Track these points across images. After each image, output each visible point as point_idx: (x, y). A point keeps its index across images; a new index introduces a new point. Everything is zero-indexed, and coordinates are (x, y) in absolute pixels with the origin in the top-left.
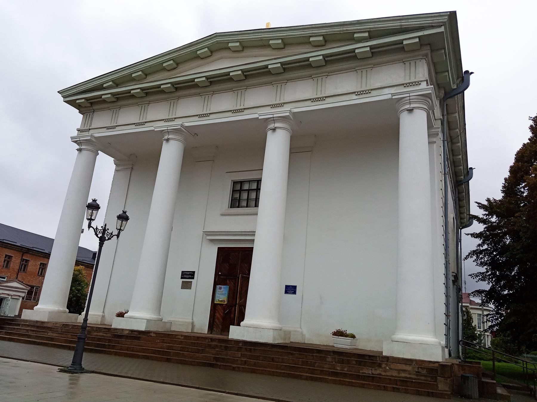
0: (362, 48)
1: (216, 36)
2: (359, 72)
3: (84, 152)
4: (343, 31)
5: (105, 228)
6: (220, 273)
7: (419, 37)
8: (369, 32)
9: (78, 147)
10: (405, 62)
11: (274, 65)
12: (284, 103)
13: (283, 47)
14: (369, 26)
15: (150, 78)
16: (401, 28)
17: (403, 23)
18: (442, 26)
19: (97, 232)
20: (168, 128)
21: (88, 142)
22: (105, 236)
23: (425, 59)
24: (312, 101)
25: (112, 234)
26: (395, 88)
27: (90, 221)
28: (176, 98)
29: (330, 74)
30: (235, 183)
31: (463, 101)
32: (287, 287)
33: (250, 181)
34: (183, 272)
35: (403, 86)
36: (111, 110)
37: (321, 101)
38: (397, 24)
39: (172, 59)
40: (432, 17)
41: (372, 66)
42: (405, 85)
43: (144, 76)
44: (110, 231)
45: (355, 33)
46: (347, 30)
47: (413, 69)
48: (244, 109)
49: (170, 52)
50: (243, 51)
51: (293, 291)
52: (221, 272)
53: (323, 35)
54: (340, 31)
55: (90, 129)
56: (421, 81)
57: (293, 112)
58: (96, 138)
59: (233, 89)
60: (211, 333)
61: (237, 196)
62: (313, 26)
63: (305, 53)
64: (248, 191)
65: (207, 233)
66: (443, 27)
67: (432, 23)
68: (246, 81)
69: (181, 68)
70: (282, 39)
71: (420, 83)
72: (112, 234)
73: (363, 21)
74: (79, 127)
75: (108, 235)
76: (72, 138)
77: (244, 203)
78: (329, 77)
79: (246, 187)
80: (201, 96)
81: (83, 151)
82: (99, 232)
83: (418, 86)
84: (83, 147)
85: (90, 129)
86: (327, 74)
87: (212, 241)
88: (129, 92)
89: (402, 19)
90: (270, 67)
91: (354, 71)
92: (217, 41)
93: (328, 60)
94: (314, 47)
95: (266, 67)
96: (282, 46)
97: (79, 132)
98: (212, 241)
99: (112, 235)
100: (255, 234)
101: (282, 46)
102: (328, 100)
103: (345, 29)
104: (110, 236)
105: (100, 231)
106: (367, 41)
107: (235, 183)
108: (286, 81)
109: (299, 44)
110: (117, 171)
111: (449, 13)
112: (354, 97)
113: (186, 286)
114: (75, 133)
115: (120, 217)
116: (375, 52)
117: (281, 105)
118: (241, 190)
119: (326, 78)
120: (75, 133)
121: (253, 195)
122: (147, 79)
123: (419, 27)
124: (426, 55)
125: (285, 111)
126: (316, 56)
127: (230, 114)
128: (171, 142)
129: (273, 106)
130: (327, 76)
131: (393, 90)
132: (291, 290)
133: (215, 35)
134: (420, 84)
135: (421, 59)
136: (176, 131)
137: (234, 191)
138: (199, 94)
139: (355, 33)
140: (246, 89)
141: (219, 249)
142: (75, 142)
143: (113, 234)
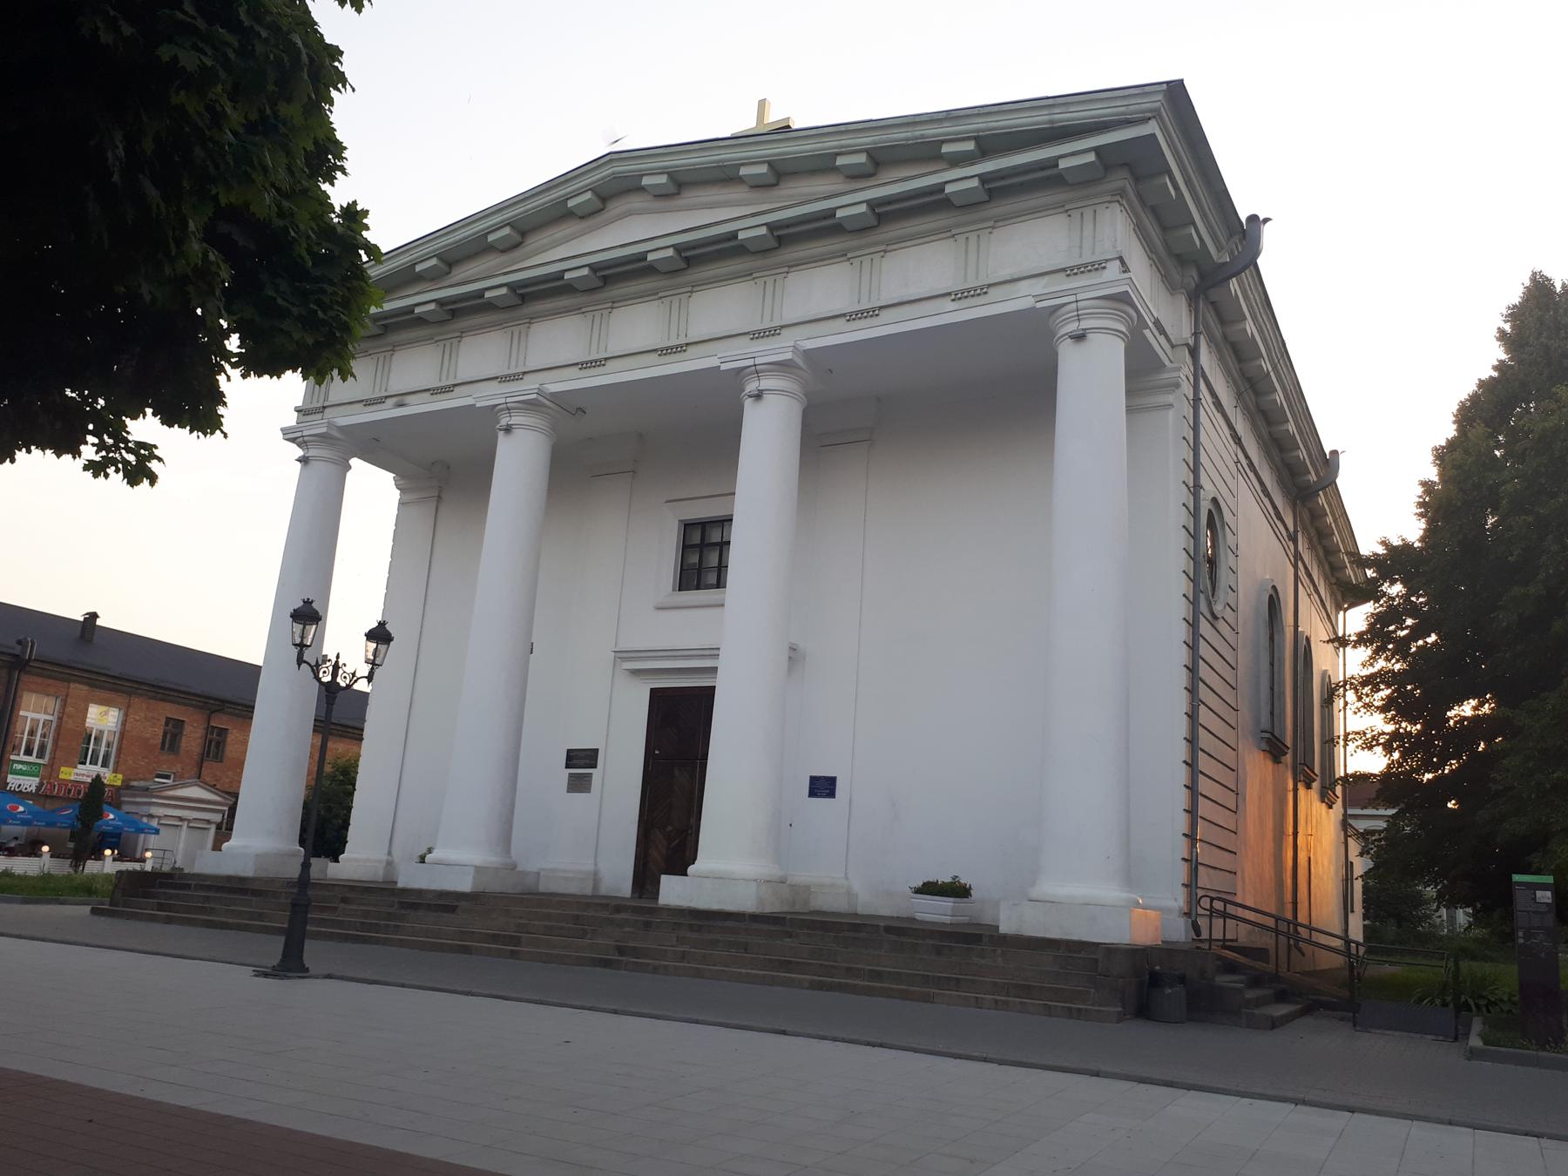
2: (961, 238)
3: (314, 465)
5: (337, 662)
6: (657, 752)
7: (1097, 150)
8: (975, 138)
9: (299, 452)
10: (1069, 213)
12: (782, 327)
13: (775, 182)
15: (461, 273)
18: (1149, 119)
19: (319, 673)
20: (509, 400)
21: (323, 438)
22: (339, 680)
23: (1118, 201)
25: (354, 674)
26: (1046, 279)
27: (301, 650)
29: (889, 248)
30: (688, 526)
31: (1260, 289)
32: (813, 780)
34: (569, 751)
35: (1063, 274)
38: (1040, 119)
39: (508, 224)
40: (1124, 97)
41: (991, 223)
42: (1069, 272)
43: (446, 269)
44: (349, 669)
45: (943, 142)
46: (922, 136)
47: (1088, 227)
48: (687, 344)
49: (502, 206)
50: (679, 194)
51: (828, 791)
52: (658, 750)
54: (907, 139)
55: (324, 407)
56: (1107, 261)
57: (804, 351)
58: (341, 429)
59: (660, 295)
60: (640, 897)
61: (694, 559)
62: (842, 128)
65: (622, 655)
66: (1153, 123)
67: (1123, 114)
68: (690, 271)
69: (534, 242)
70: (770, 163)
71: (1104, 265)
72: (354, 674)
74: (299, 403)
75: (345, 677)
78: (888, 254)
80: (583, 313)
81: (313, 462)
82: (325, 672)
83: (1099, 272)
84: (312, 453)
85: (324, 407)
86: (883, 247)
88: (409, 310)
90: (741, 236)
91: (948, 237)
92: (613, 173)
93: (885, 214)
95: (733, 235)
96: (772, 180)
99: (355, 678)
100: (718, 655)
101: (772, 180)
102: (886, 315)
103: (918, 133)
104: (350, 681)
105: (325, 669)
106: (973, 164)
107: (688, 526)
108: (786, 269)
110: (401, 503)
111: (1165, 86)
112: (947, 304)
113: (579, 784)
115: (370, 636)
117: (773, 332)
119: (882, 257)
120: (291, 420)
122: (450, 275)
124: (1122, 193)
126: (852, 203)
127: (654, 357)
128: (517, 433)
129: (757, 335)
130: (885, 251)
131: (1039, 286)
132: (823, 787)
134: (1104, 268)
135: (1110, 202)
136: (530, 406)
137: (686, 547)
138: (577, 310)
139: (943, 142)
140: (692, 292)
141: (654, 692)
142: (293, 440)
143: (358, 675)
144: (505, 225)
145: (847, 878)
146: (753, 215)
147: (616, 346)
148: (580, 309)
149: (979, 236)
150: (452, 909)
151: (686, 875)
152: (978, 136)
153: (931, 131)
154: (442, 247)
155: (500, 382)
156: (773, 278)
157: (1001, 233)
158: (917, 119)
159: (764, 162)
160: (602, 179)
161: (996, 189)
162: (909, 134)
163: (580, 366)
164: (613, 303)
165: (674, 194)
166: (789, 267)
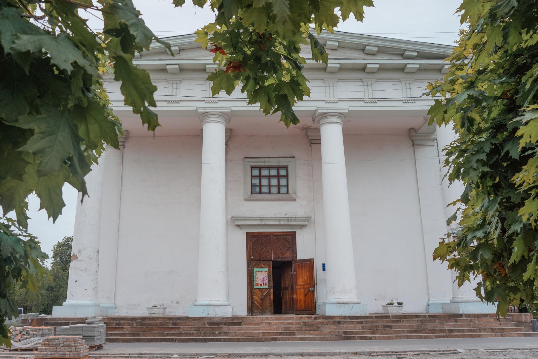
0: (413, 64)
4: (396, 47)
6: (252, 258)
14: (419, 48)
15: (184, 55)
24: (326, 103)
28: (179, 80)
29: (378, 80)
33: (269, 168)
37: (409, 103)
46: (400, 47)
54: (394, 46)
64: (269, 177)
65: (234, 219)
73: (412, 42)
79: (265, 172)
87: (238, 226)
89: (445, 48)
93: (383, 69)
94: (365, 54)
98: (238, 226)
109: (350, 49)
112: (401, 103)
118: (260, 177)
121: (283, 182)
125: (343, 107)
145: (115, 304)
146: (335, 59)
147: (378, 95)
149: (329, 83)
151: (62, 306)
153: (404, 46)
155: (206, 103)
156: (332, 82)
157: (340, 83)
158: (399, 41)
159: (337, 41)
162: (395, 45)
163: (168, 102)
164: (415, 79)
166: (415, 79)
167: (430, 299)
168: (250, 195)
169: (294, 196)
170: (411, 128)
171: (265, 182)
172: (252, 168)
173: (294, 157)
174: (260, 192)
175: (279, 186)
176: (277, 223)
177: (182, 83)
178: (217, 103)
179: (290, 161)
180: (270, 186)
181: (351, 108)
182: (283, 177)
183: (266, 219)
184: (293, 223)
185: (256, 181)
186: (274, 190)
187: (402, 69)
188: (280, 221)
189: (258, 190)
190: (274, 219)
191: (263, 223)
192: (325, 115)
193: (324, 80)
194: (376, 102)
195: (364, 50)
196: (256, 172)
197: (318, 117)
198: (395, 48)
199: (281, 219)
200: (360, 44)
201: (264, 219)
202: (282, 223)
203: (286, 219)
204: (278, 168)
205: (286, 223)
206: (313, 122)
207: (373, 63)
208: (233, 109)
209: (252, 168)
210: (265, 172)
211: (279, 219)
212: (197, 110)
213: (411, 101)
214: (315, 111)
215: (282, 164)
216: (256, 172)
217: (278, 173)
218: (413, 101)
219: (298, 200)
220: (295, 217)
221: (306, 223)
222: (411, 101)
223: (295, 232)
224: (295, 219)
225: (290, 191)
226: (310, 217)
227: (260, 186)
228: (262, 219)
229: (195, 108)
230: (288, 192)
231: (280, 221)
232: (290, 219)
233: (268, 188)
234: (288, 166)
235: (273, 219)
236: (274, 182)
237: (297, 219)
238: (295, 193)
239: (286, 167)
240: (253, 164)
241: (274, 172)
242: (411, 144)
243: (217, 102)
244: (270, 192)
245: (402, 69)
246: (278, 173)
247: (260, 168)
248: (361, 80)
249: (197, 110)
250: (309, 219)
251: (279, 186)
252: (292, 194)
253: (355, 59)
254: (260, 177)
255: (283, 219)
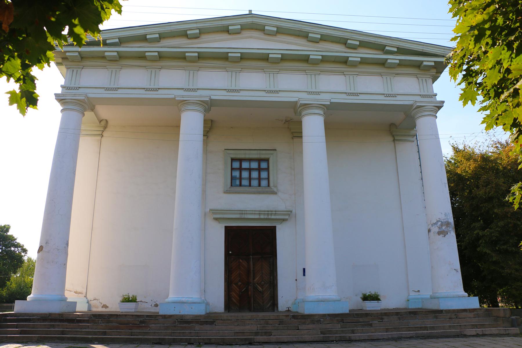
0: (393, 59)
1: (252, 17)
6: (230, 252)
7: (435, 62)
8: (397, 48)
10: (418, 78)
11: (315, 56)
14: (399, 44)
15: (165, 42)
16: (422, 52)
17: (424, 49)
33: (250, 160)
36: (108, 69)
38: (419, 48)
40: (444, 49)
49: (197, 21)
50: (275, 35)
53: (360, 41)
59: (265, 70)
63: (345, 52)
64: (250, 170)
65: (214, 211)
67: (444, 54)
70: (321, 35)
76: (56, 95)
77: (245, 182)
79: (245, 165)
93: (364, 62)
97: (64, 89)
108: (320, 72)
109: (333, 42)
114: (59, 91)
116: (402, 64)
118: (241, 169)
120: (59, 91)
121: (264, 175)
123: (435, 54)
125: (326, 99)
126: (355, 56)
133: (251, 15)
135: (430, 78)
141: (226, 227)
144: (197, 29)
146: (317, 51)
148: (226, 68)
150: (212, 323)
152: (399, 48)
153: (384, 42)
154: (162, 31)
160: (247, 22)
161: (402, 64)
162: (376, 40)
165: (274, 35)
167: (411, 294)
168: (230, 188)
169: (275, 190)
170: (392, 124)
171: (245, 174)
172: (233, 160)
173: (275, 150)
174: (241, 185)
175: (259, 179)
176: (257, 217)
177: (162, 70)
178: (196, 91)
179: (272, 154)
180: (250, 179)
181: (332, 101)
182: (264, 169)
183: (245, 212)
184: (273, 217)
185: (236, 174)
186: (255, 183)
187: (383, 63)
188: (260, 215)
189: (238, 182)
190: (254, 212)
191: (243, 216)
192: (306, 106)
193: (306, 72)
194: (358, 95)
195: (346, 44)
196: (236, 165)
197: (299, 107)
198: (376, 43)
199: (261, 212)
200: (341, 38)
201: (244, 212)
202: (262, 217)
203: (266, 212)
204: (260, 160)
205: (266, 217)
206: (295, 114)
207: (355, 56)
208: (213, 97)
209: (233, 160)
210: (245, 165)
211: (259, 212)
212: (175, 98)
213: (392, 96)
214: (296, 102)
215: (263, 157)
216: (236, 165)
217: (259, 165)
218: (394, 96)
219: (280, 194)
220: (276, 211)
221: (287, 217)
222: (392, 96)
223: (275, 227)
224: (276, 212)
225: (271, 184)
226: (291, 211)
227: (241, 178)
228: (242, 212)
229: (173, 96)
230: (269, 186)
231: (260, 215)
232: (270, 213)
233: (249, 181)
234: (269, 158)
235: (253, 212)
236: (255, 174)
237: (277, 213)
238: (276, 187)
239: (267, 160)
240: (233, 156)
241: (255, 165)
242: (392, 139)
243: (196, 90)
244: (250, 185)
245: (383, 63)
246: (259, 165)
247: (241, 160)
248: (343, 73)
249: (175, 98)
250: (290, 213)
251: (259, 179)
252: (272, 188)
253: (336, 52)
254: (241, 169)
255: (263, 212)
